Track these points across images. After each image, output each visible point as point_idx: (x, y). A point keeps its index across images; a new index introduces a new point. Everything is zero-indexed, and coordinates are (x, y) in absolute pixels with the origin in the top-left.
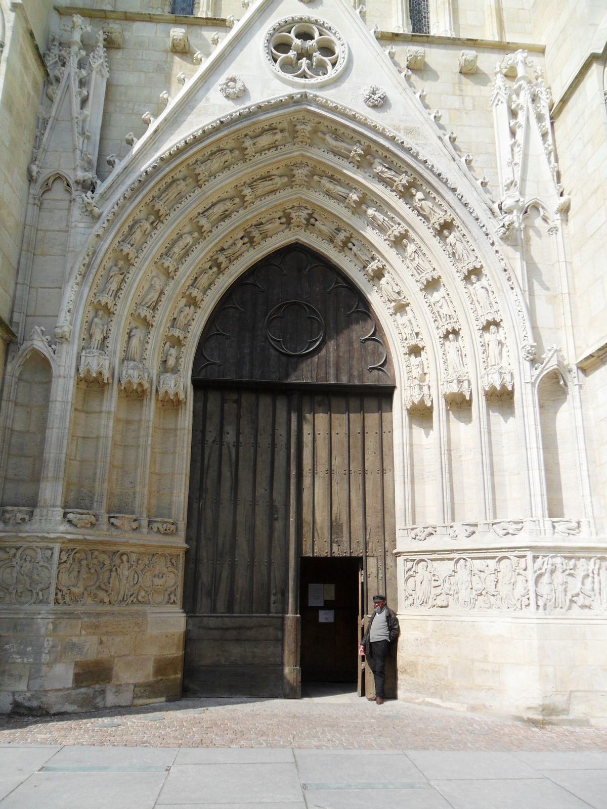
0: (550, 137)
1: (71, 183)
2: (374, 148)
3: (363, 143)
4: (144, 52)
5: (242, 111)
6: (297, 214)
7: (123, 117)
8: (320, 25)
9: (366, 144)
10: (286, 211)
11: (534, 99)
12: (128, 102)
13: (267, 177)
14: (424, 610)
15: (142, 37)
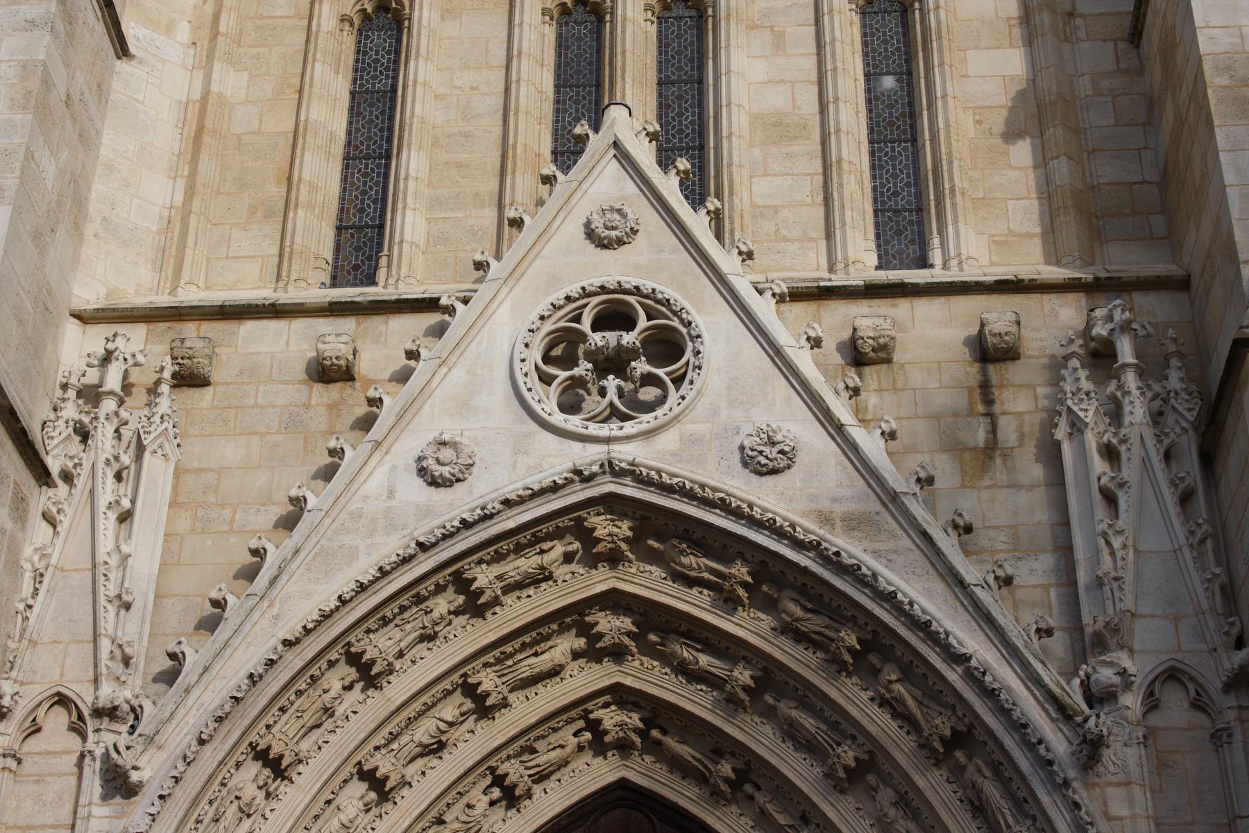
0: (1200, 498)
1: (86, 712)
3: (750, 558)
4: (261, 388)
5: (464, 516)
6: (618, 719)
7: (209, 542)
8: (646, 297)
9: (757, 560)
10: (591, 716)
12: (222, 506)
15: (258, 354)
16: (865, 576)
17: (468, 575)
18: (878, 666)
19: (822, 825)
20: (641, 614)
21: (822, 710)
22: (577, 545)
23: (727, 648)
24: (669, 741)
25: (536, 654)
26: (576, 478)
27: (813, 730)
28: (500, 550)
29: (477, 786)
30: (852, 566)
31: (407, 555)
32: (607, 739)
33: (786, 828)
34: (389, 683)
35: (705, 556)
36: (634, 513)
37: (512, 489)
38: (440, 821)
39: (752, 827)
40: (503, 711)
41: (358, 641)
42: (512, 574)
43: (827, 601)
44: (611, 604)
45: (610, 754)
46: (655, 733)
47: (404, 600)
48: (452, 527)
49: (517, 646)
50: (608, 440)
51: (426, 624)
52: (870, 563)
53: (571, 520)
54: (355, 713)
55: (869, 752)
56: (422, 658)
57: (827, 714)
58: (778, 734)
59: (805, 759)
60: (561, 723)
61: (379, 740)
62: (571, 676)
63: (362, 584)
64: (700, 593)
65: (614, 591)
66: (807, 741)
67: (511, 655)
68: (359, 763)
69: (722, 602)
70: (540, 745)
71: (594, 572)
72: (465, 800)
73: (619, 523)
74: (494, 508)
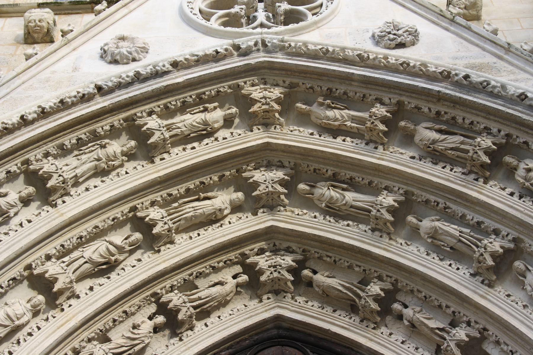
2: (411, 103)
10: (248, 261)
16: (494, 87)
17: (139, 122)
18: (515, 163)
19: (473, 320)
20: (292, 169)
21: (463, 216)
22: (234, 110)
23: (370, 183)
24: (320, 278)
25: (198, 200)
26: (235, 53)
27: (457, 234)
28: (169, 105)
29: (142, 312)
30: (481, 83)
31: (86, 92)
32: (263, 278)
33: (437, 331)
34: (64, 202)
35: (346, 108)
36: (284, 82)
38: (104, 338)
39: (403, 343)
40: (168, 246)
41: (37, 161)
42: (179, 125)
43: (460, 121)
44: (265, 162)
45: (265, 297)
46: (306, 272)
47: (82, 133)
48: (128, 76)
49: (182, 191)
51: (101, 156)
53: (230, 87)
54: (29, 221)
55: (515, 240)
56: (95, 187)
57: (469, 217)
58: (422, 249)
59: (450, 265)
60: (221, 264)
61: (51, 248)
62: (230, 223)
63: (43, 109)
64: (344, 141)
65: (267, 146)
66: (451, 248)
67: (176, 200)
68: (29, 267)
69: (364, 144)
70: (201, 283)
71: (250, 133)
72: (129, 322)
73: (272, 90)
74: (164, 66)
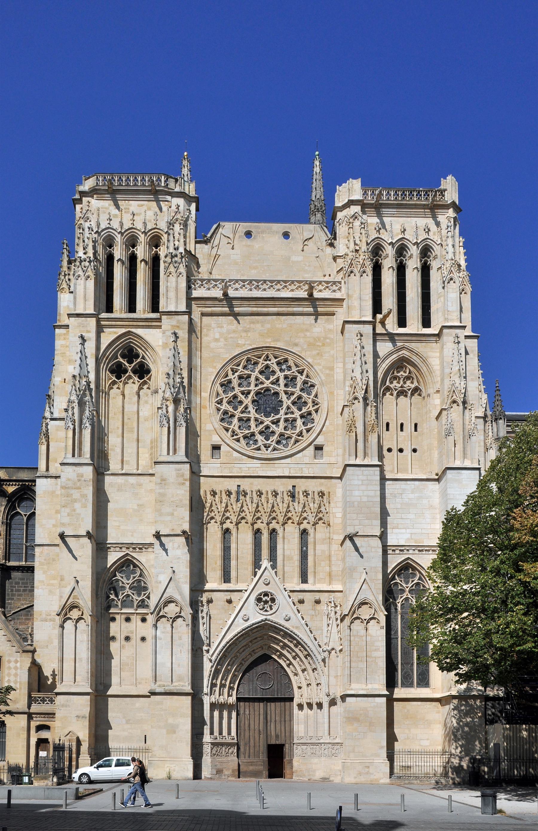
11: (336, 613)
13: (256, 638)
14: (299, 757)
37: (254, 622)
50: (266, 615)
52: (298, 634)
